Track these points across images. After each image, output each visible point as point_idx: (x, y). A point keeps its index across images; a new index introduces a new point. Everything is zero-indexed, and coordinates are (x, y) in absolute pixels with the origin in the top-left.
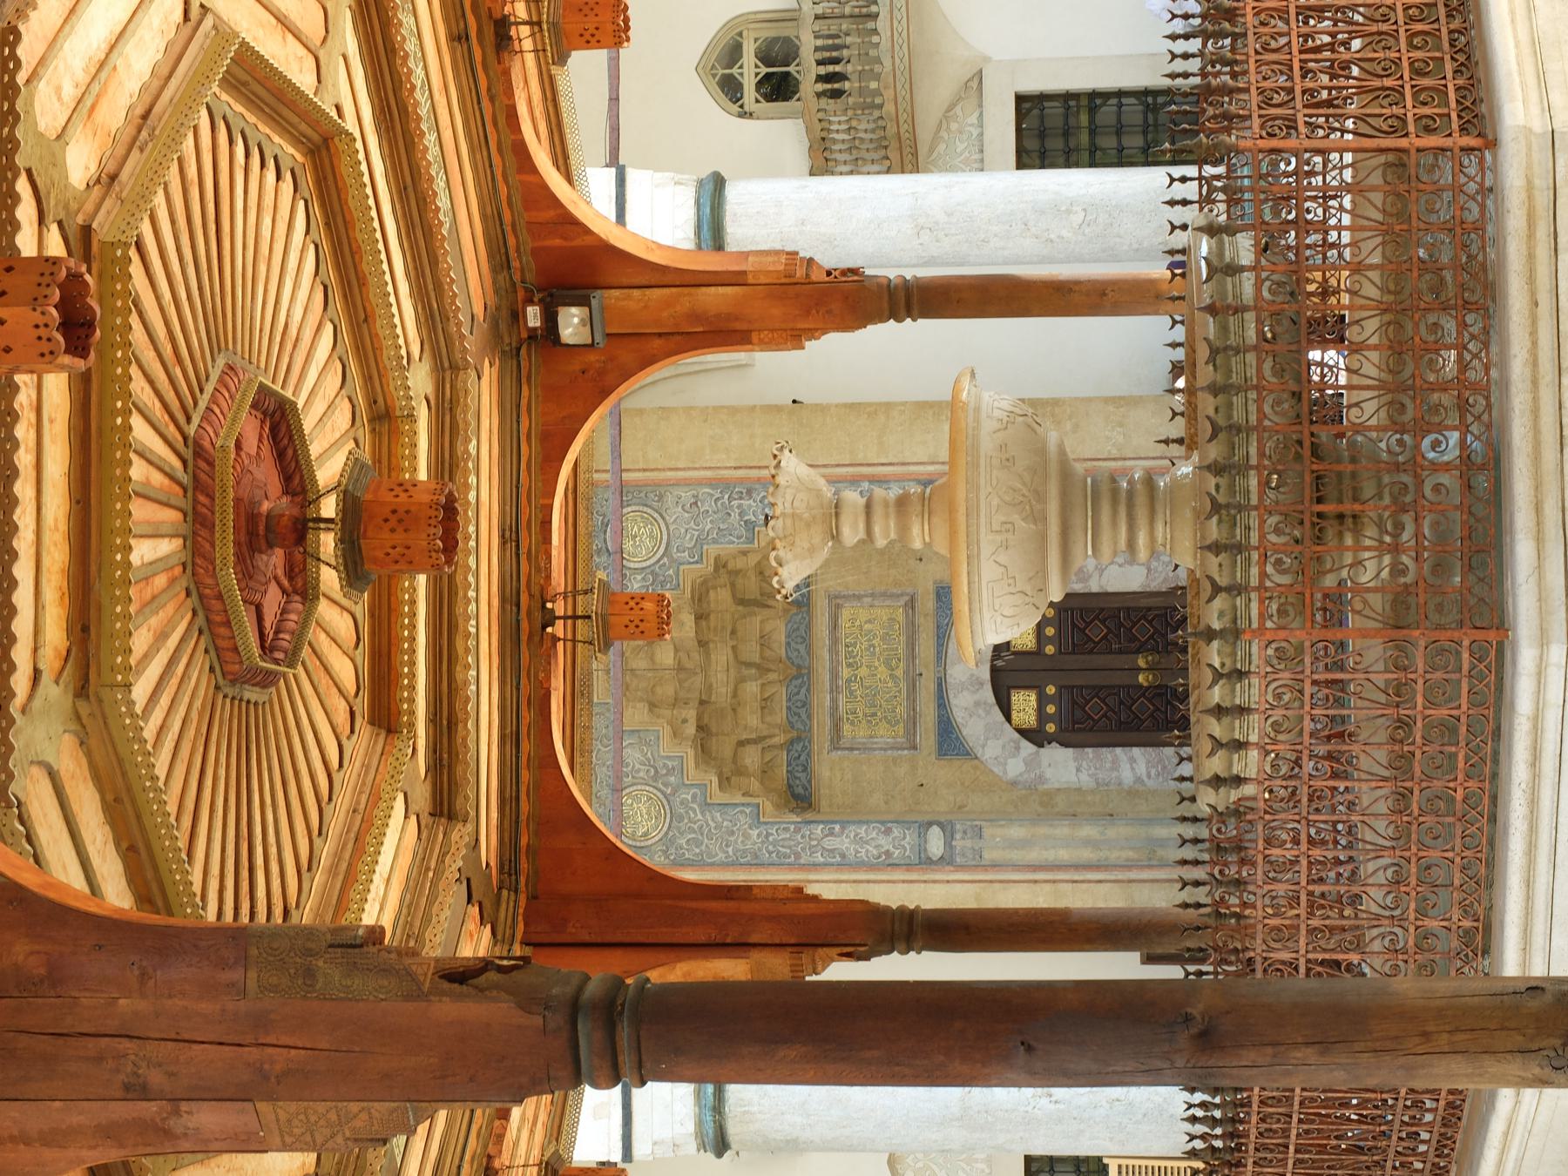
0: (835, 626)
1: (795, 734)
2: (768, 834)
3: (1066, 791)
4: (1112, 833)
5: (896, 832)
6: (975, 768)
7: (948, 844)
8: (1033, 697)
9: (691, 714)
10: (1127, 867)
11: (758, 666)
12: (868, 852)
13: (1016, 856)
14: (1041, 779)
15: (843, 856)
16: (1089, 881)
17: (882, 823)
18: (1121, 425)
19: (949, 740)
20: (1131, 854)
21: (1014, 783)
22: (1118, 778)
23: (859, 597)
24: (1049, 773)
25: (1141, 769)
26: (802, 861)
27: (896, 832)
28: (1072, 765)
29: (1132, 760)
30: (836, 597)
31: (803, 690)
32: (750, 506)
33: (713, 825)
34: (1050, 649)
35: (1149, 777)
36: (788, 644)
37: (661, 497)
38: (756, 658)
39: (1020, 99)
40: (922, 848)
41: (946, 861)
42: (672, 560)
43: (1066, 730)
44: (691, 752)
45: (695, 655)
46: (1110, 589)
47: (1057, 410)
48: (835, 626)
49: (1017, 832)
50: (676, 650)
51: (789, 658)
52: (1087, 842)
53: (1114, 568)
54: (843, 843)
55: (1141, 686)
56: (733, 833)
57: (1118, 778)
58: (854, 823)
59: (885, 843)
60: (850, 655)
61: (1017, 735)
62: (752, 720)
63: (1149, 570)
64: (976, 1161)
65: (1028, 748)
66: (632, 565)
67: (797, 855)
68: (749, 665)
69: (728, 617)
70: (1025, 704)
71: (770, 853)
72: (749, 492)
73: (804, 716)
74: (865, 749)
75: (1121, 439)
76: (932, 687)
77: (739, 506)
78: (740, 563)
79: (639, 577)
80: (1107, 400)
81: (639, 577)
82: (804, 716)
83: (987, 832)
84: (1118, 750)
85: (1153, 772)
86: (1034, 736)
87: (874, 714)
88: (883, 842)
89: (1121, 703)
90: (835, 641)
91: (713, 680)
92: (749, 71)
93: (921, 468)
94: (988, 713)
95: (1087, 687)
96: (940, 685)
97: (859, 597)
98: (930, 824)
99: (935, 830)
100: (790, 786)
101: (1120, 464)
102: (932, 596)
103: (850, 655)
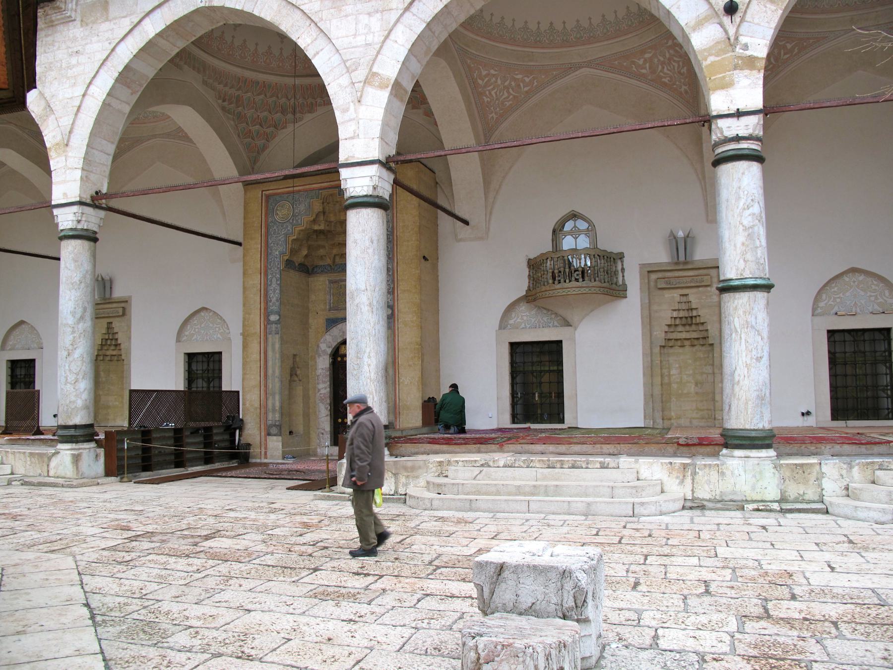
4: (277, 380)
7: (273, 322)
9: (322, 227)
14: (319, 356)
21: (318, 346)
24: (321, 358)
25: (323, 391)
27: (277, 304)
29: (325, 388)
40: (272, 313)
41: (268, 322)
49: (277, 346)
52: (274, 372)
59: (274, 300)
65: (329, 351)
83: (277, 336)
99: (278, 318)
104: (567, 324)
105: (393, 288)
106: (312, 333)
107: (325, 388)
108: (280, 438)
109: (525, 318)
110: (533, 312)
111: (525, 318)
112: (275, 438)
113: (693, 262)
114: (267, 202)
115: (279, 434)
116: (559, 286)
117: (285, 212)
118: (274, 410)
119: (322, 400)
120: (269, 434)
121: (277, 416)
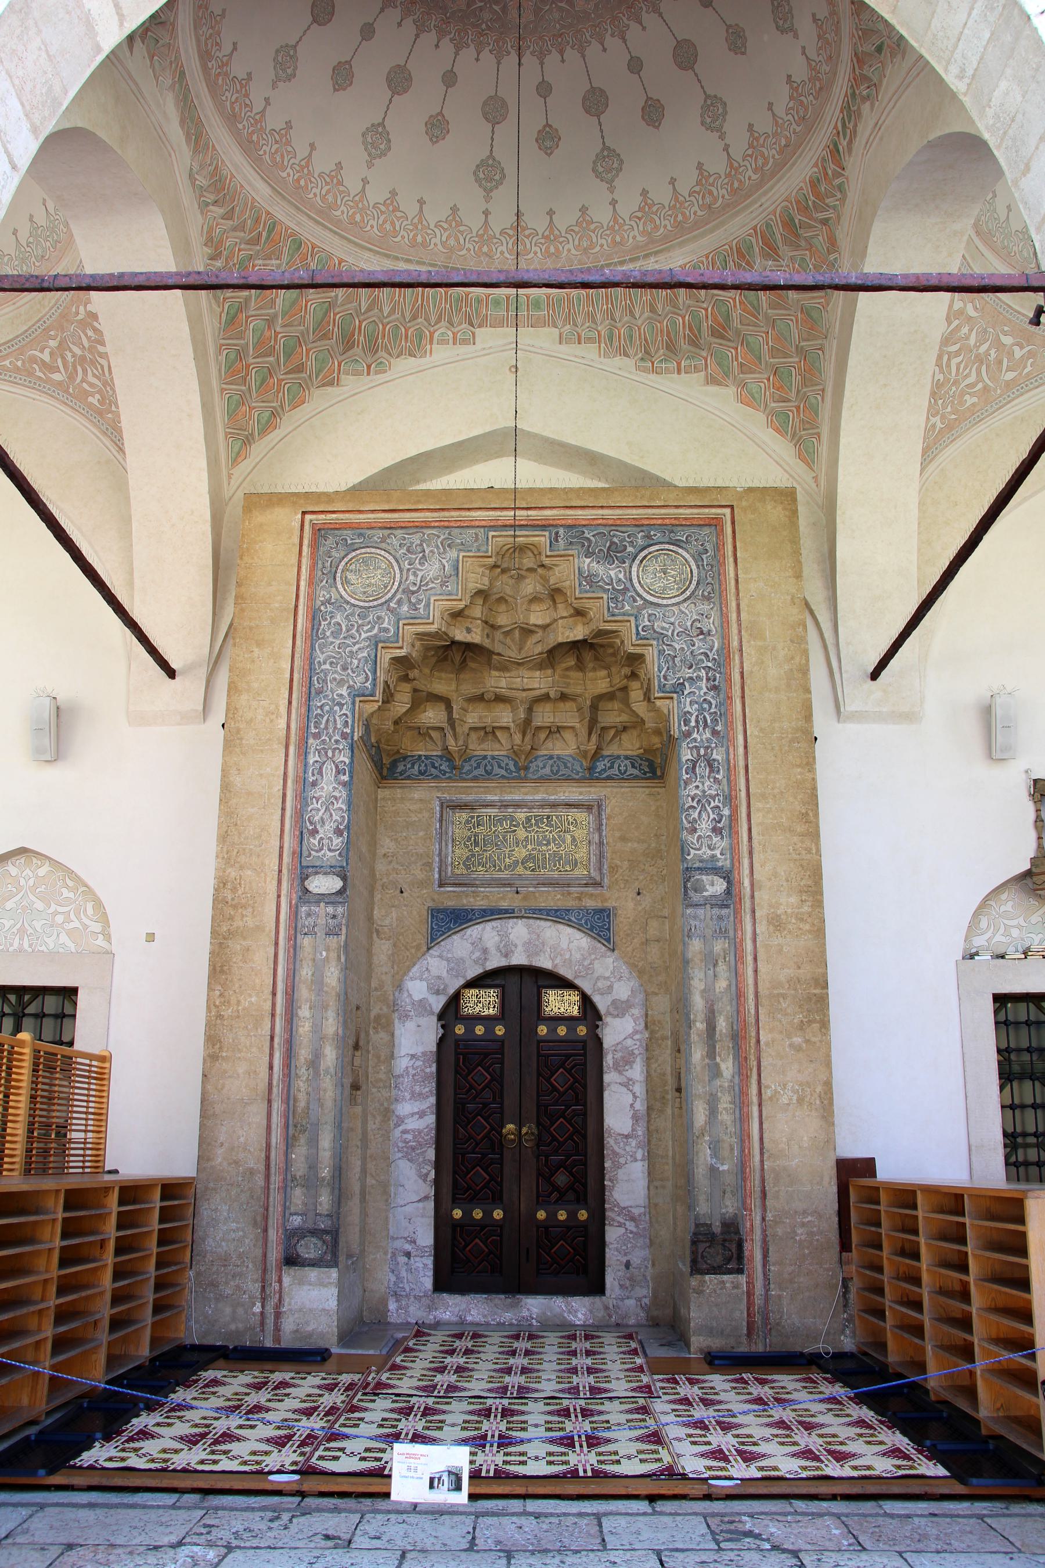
0: (569, 805)
1: (458, 763)
2: (341, 705)
3: (392, 1044)
5: (337, 841)
6: (418, 947)
7: (321, 898)
8: (492, 1012)
9: (476, 637)
10: (288, 1098)
11: (528, 722)
12: (317, 811)
13: (306, 972)
15: (314, 784)
16: (271, 1055)
17: (348, 827)
18: (800, 1101)
19: (448, 920)
20: (302, 1104)
21: (399, 987)
22: (404, 1099)
23: (599, 829)
24: (410, 1025)
25: (413, 1124)
26: (311, 741)
27: (337, 841)
28: (419, 1050)
29: (422, 1114)
30: (599, 806)
31: (503, 772)
32: (700, 689)
33: (355, 649)
34: (543, 1030)
35: (405, 1132)
36: (551, 757)
37: (708, 599)
38: (538, 721)
40: (318, 870)
42: (640, 609)
43: (457, 1045)
44: (433, 628)
45: (539, 649)
46: (606, 1094)
47: (816, 1026)
48: (569, 805)
49: (333, 976)
50: (545, 627)
51: (536, 758)
53: (630, 1098)
54: (328, 785)
55: (503, 1126)
56: (345, 669)
57: (404, 1099)
58: (349, 796)
59: (326, 831)
60: (539, 820)
61: (451, 991)
62: (474, 717)
63: (627, 1137)
64: (22, 939)
65: (438, 1003)
66: (634, 569)
67: (317, 736)
68: (530, 710)
69: (579, 690)
70: (484, 1003)
71: (321, 707)
72: (715, 688)
73: (476, 773)
74: (442, 834)
75: (785, 1100)
76: (504, 904)
77: (699, 678)
78: (636, 694)
79: (621, 576)
80: (828, 1084)
81: (621, 576)
82: (476, 773)
83: (333, 941)
84: (433, 1100)
85: (410, 1137)
86: (451, 1011)
87: (476, 844)
88: (327, 827)
89: (485, 1105)
90: (554, 805)
91: (513, 674)
93: (746, 871)
94: (476, 962)
95: (502, 1069)
96: (506, 911)
97: (599, 829)
98: (344, 878)
99: (337, 884)
100: (405, 758)
101: (755, 1099)
102: (599, 905)
103: (539, 820)
105: (733, 818)
106: (382, 949)
107: (422, 1114)
108: (334, 1273)
109: (1015, 933)
110: (1035, 918)
111: (1015, 933)
112: (313, 1274)
114: (315, 545)
115: (330, 1259)
117: (377, 577)
118: (310, 1182)
119: (410, 1152)
120: (291, 1260)
121: (325, 1201)
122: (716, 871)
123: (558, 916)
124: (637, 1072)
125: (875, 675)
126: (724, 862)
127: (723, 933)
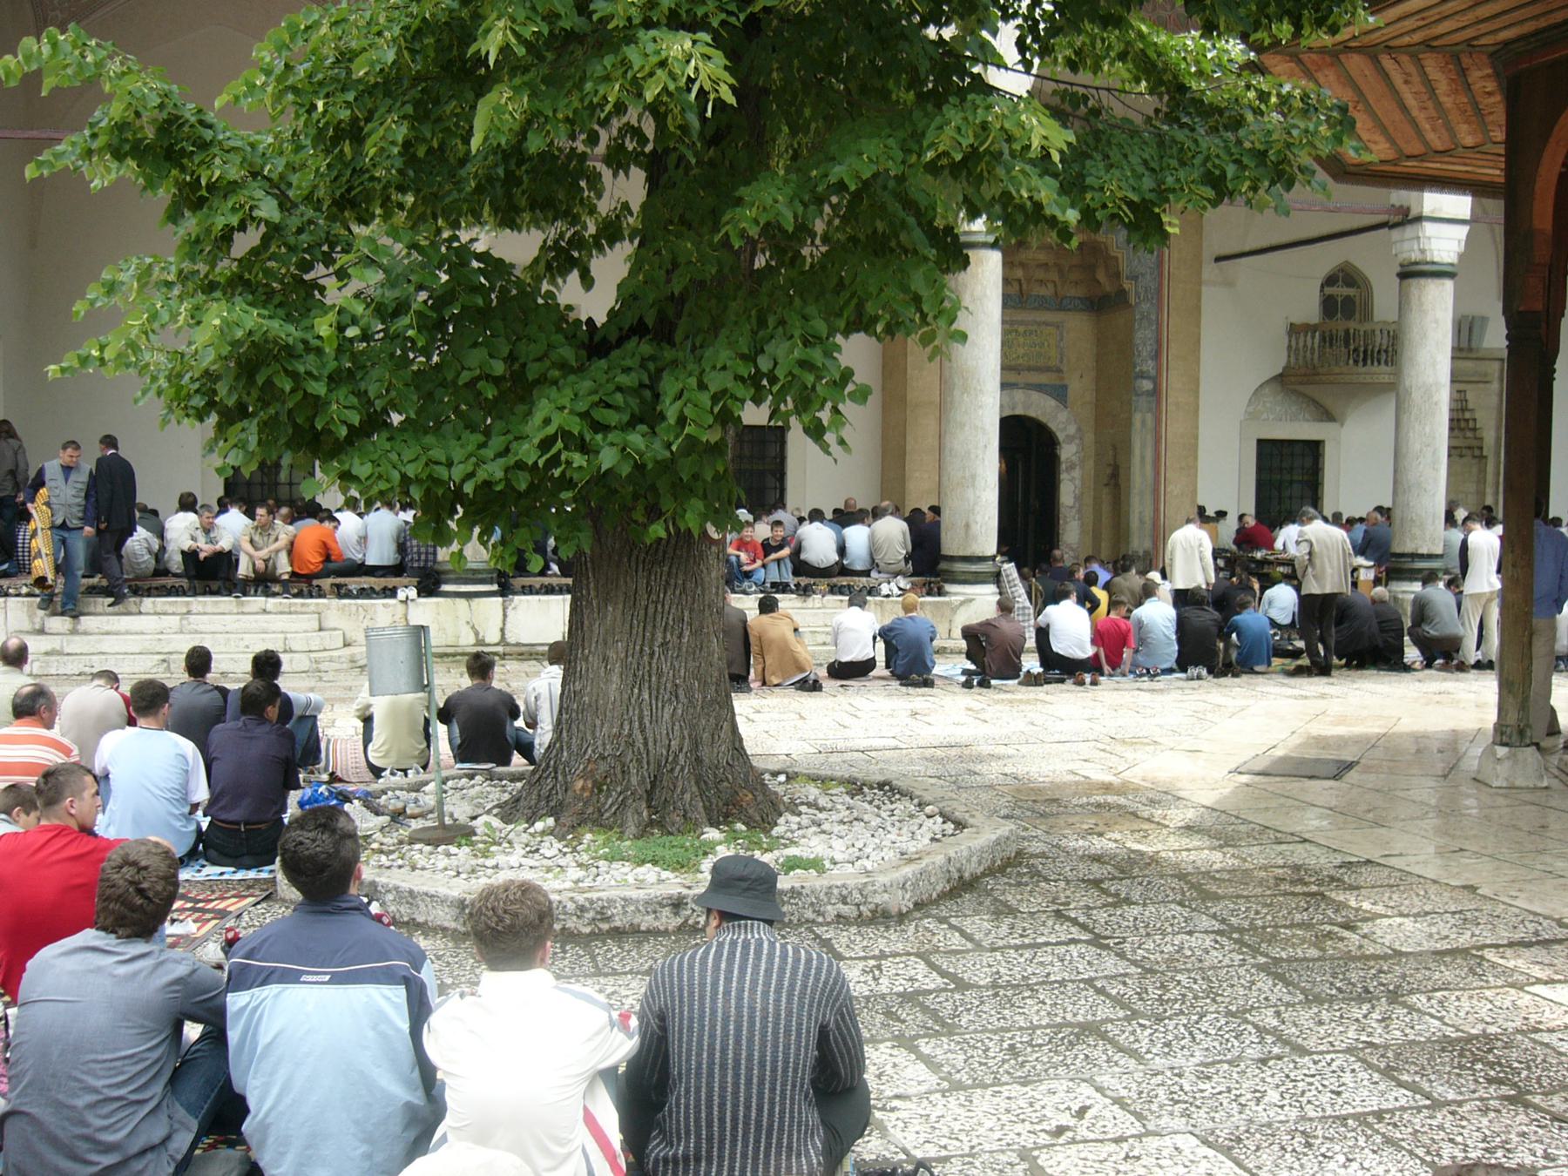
0: (1047, 324)
39: (1260, 442)
48: (1047, 324)
90: (1039, 324)
92: (1340, 291)
104: (1327, 416)
113: (1478, 350)
116: (1364, 370)
122: (1148, 378)
123: (1039, 388)
124: (1076, 473)
125: (1218, 259)
126: (1153, 373)
127: (1150, 410)
